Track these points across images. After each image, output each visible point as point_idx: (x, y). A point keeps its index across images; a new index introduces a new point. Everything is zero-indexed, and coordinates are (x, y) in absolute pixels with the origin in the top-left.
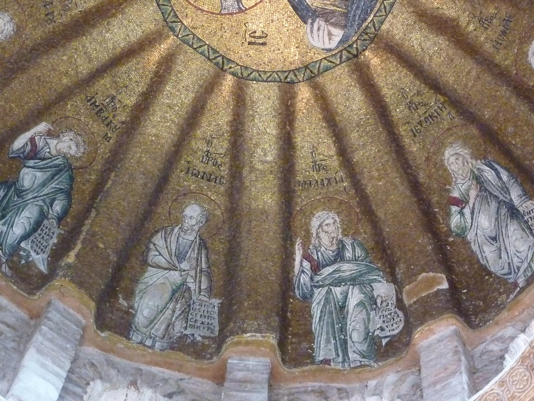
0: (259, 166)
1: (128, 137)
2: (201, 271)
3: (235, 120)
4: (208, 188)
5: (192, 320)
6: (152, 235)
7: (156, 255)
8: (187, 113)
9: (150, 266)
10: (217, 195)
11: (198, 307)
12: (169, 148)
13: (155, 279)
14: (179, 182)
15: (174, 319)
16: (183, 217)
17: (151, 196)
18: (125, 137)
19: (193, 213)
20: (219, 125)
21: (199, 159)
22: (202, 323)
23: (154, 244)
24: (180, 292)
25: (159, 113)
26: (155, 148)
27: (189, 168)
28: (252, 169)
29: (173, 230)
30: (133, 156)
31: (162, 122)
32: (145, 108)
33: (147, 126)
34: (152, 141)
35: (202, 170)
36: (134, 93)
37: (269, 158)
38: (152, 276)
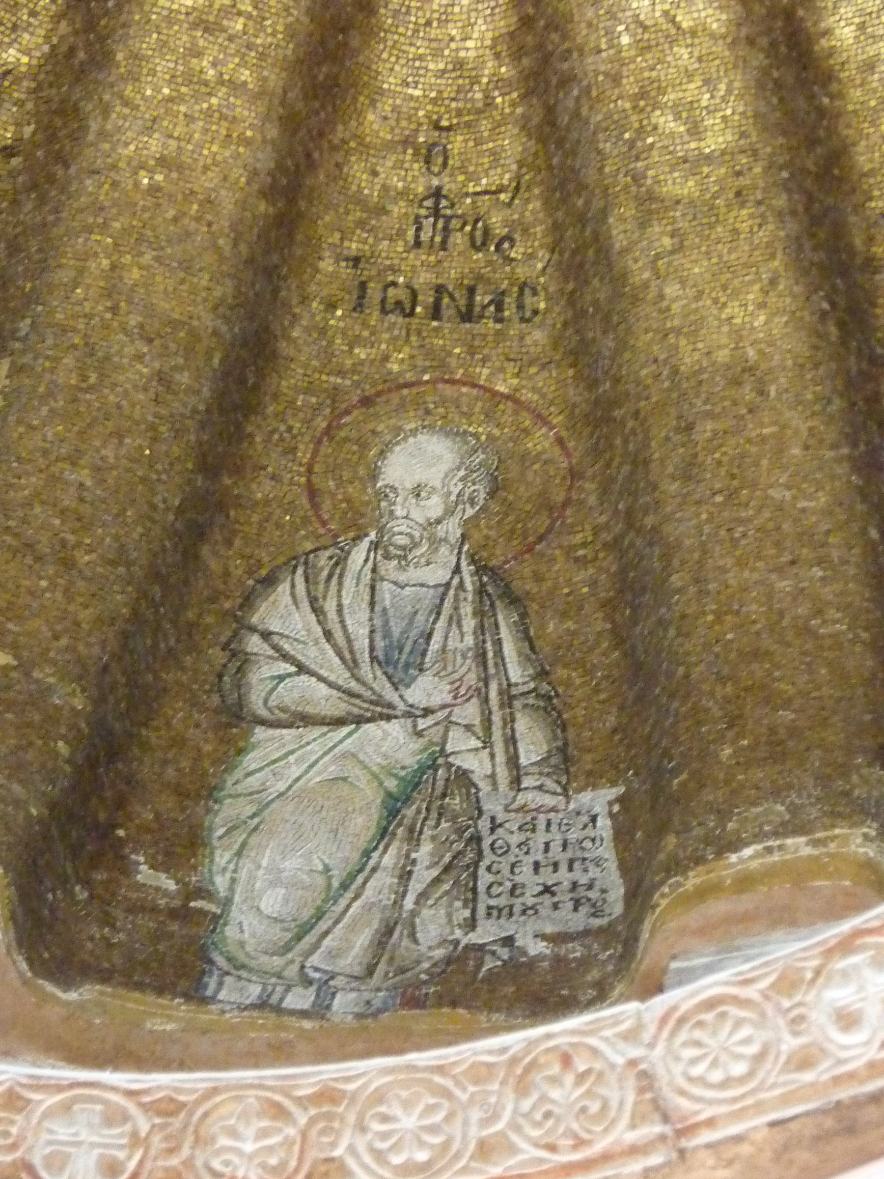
0: (679, 186)
1: (42, 200)
2: (508, 698)
3: (526, 22)
4: (472, 350)
5: (495, 890)
6: (248, 601)
7: (281, 678)
8: (291, 33)
9: (263, 722)
10: (519, 365)
11: (514, 840)
12: (243, 205)
13: (295, 772)
14: (328, 354)
15: (409, 903)
16: (381, 495)
17: (203, 425)
18: (29, 206)
19: (424, 473)
20: (459, 64)
21: (401, 233)
22: (547, 890)
23: (266, 635)
24: (423, 796)
25: (163, 65)
26: (175, 220)
27: (363, 286)
28: (651, 206)
29: (340, 562)
30: (81, 271)
31: (181, 99)
32: (92, 60)
33: (119, 129)
34: (154, 190)
35: (424, 278)
36: (33, 14)
37: (715, 141)
38: (273, 762)
